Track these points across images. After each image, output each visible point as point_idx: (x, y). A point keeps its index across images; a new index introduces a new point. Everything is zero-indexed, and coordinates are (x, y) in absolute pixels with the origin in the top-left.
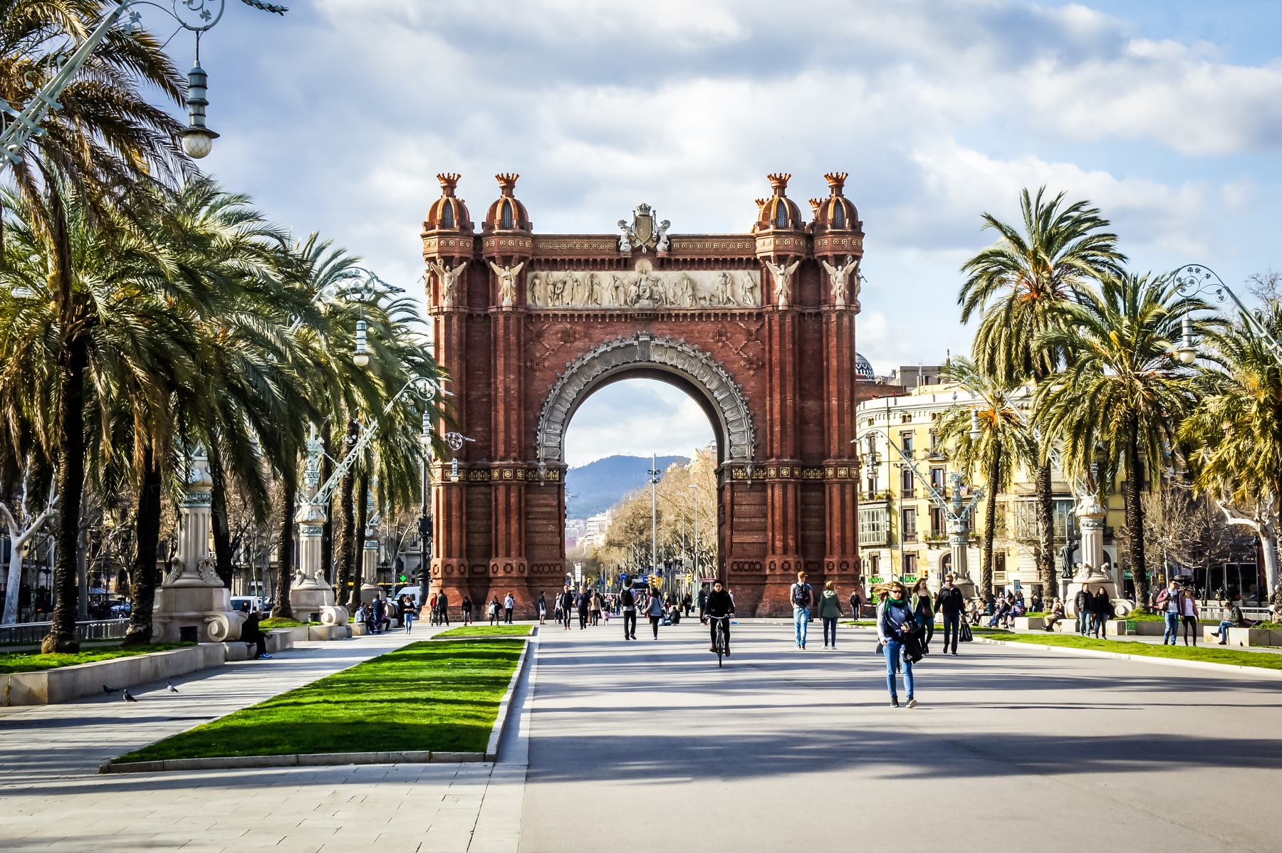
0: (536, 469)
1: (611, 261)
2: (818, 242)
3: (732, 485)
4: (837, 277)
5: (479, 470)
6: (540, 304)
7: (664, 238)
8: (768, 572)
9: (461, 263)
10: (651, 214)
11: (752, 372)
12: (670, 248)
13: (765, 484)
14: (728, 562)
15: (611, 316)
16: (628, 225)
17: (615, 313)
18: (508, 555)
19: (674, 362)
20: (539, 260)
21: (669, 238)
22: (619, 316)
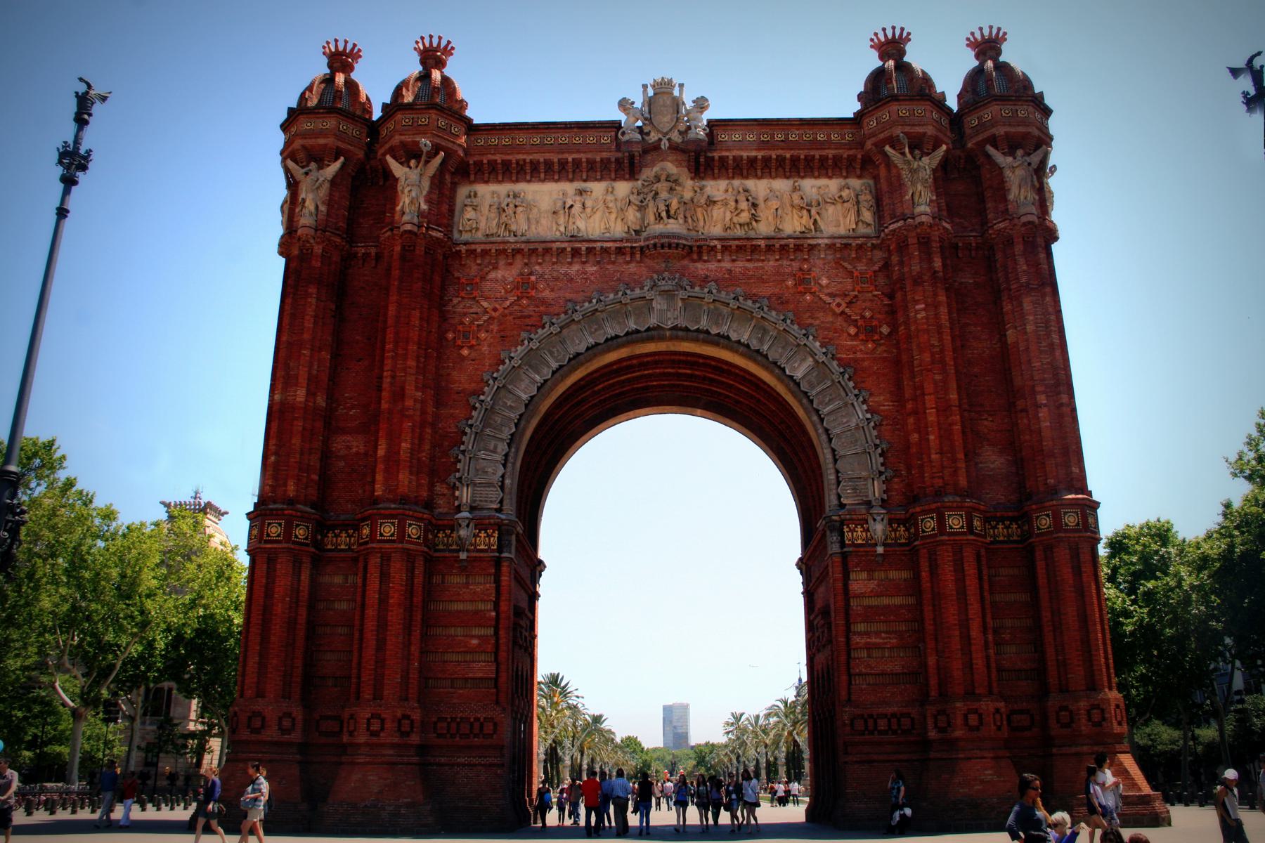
0: (454, 526)
1: (605, 163)
3: (844, 556)
4: (1013, 169)
5: (345, 526)
6: (479, 236)
8: (932, 734)
9: (336, 159)
10: (676, 93)
12: (711, 135)
14: (846, 714)
15: (605, 251)
16: (638, 105)
18: (378, 695)
19: (724, 330)
20: (479, 164)
21: (712, 124)
22: (620, 251)
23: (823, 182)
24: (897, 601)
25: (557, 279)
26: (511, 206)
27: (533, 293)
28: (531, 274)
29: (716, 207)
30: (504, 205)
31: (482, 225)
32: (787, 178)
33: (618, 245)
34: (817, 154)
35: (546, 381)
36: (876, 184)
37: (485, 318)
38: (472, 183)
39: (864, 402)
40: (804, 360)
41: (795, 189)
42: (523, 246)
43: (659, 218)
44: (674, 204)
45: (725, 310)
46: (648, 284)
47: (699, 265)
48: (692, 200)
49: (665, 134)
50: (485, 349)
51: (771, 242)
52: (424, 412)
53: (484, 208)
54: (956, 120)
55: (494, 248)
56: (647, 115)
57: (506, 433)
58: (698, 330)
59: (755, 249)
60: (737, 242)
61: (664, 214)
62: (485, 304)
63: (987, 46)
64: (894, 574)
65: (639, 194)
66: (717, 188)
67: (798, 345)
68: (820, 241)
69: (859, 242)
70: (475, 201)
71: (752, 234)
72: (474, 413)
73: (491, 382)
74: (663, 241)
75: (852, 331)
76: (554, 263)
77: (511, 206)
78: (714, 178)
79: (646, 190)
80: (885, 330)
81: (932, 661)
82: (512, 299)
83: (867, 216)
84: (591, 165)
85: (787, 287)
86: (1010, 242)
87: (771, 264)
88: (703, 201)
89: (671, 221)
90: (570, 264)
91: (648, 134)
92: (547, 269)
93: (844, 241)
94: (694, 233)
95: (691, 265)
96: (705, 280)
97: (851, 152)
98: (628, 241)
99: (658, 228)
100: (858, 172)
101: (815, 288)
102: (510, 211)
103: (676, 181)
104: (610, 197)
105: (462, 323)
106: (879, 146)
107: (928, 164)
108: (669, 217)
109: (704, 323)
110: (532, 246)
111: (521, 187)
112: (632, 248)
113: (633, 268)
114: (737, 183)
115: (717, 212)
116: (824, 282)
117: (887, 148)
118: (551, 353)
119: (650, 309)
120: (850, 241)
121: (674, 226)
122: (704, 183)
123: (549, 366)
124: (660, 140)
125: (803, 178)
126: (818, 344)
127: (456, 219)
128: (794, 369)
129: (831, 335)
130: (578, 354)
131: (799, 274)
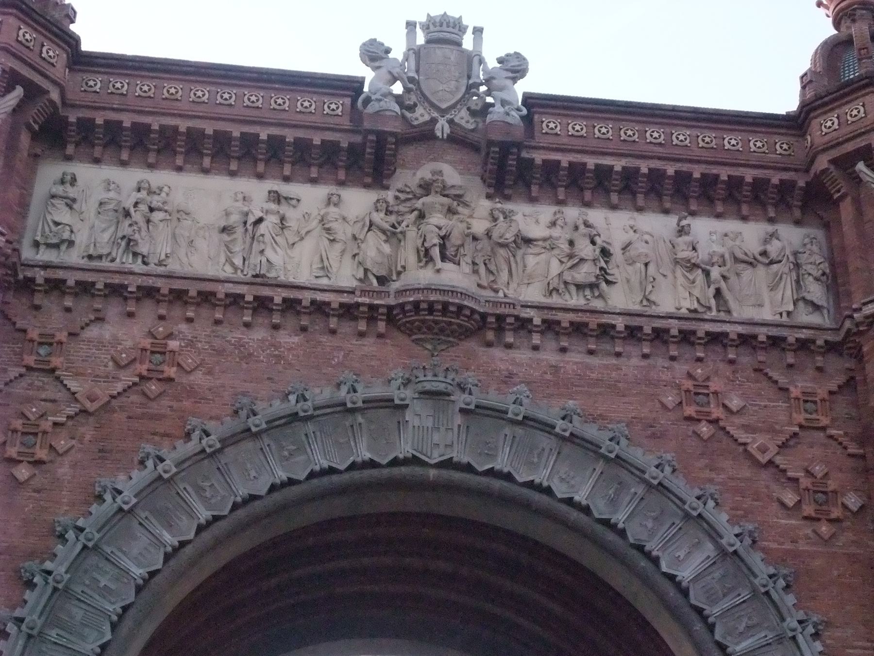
10: (468, 42)
11: (824, 529)
15: (320, 308)
16: (398, 53)
17: (335, 299)
19: (541, 477)
20: (86, 127)
22: (348, 311)
23: (731, 225)
25: (220, 352)
26: (143, 208)
27: (172, 372)
28: (170, 336)
29: (533, 250)
30: (129, 204)
31: (81, 238)
32: (666, 212)
33: (345, 299)
34: (724, 173)
35: (183, 544)
36: (829, 239)
37: (71, 411)
38: (68, 158)
39: (816, 636)
40: (697, 545)
41: (682, 231)
42: (159, 283)
43: (425, 256)
44: (455, 240)
45: (545, 441)
46: (399, 373)
47: (497, 352)
48: (488, 234)
49: (443, 112)
51: (635, 322)
53: (86, 207)
55: (100, 281)
56: (412, 74)
58: (491, 473)
59: (606, 331)
60: (571, 316)
61: (436, 252)
62: (73, 385)
65: (388, 212)
66: (533, 218)
67: (687, 516)
68: (727, 328)
69: (803, 334)
70: (72, 192)
71: (598, 304)
72: (28, 595)
73: (71, 535)
74: (433, 297)
75: (790, 498)
76: (218, 322)
77: (143, 208)
78: (533, 200)
79: (401, 208)
80: (853, 501)
82: (127, 378)
83: (816, 292)
84: (302, 148)
85: (664, 406)
87: (632, 363)
88: (510, 236)
89: (449, 266)
90: (247, 325)
91: (412, 108)
92: (202, 330)
93: (774, 332)
94: (488, 294)
95: (481, 350)
96: (508, 379)
97: (786, 176)
98: (364, 292)
100: (797, 213)
101: (717, 412)
102: (137, 216)
103: (458, 197)
104: (332, 209)
105: (23, 416)
106: (845, 163)
108: (444, 258)
109: (502, 463)
110: (177, 285)
112: (372, 308)
113: (369, 346)
114: (572, 213)
115: (533, 260)
116: (735, 403)
117: (861, 166)
118: (199, 490)
119: (401, 424)
120: (784, 332)
121: (454, 276)
122: (508, 206)
123: (191, 515)
124: (434, 121)
125: (693, 214)
126: (724, 517)
127: (31, 221)
128: (678, 561)
129: (748, 503)
130: (253, 498)
131: (688, 384)
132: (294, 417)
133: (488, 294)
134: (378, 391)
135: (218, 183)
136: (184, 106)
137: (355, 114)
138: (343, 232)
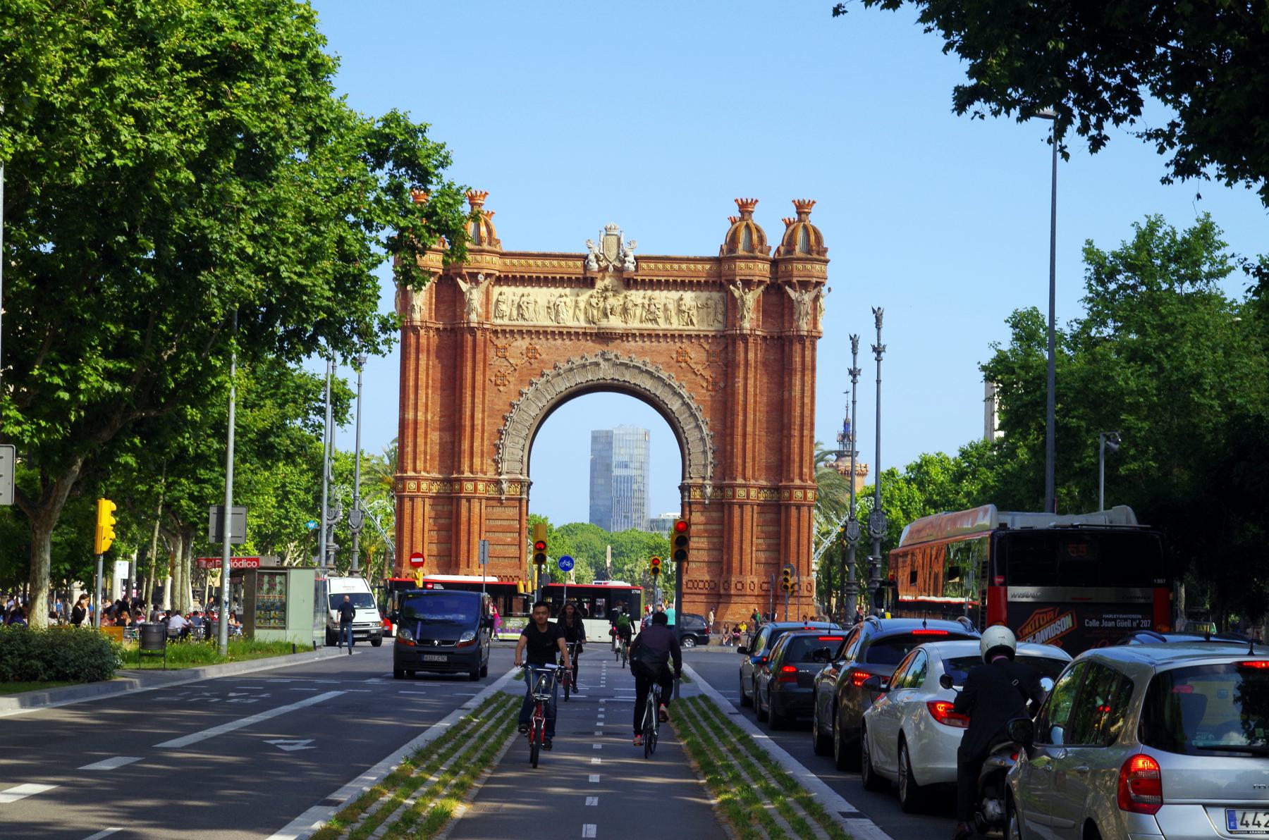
0: (498, 483)
2: (782, 267)
6: (506, 321)
7: (631, 258)
8: (722, 591)
12: (637, 267)
13: (723, 504)
15: (577, 334)
17: (581, 331)
20: (506, 277)
22: (585, 334)
23: (698, 293)
24: (714, 527)
34: (695, 280)
50: (512, 387)
52: (483, 425)
54: (774, 263)
57: (524, 434)
59: (657, 335)
63: (802, 208)
64: (714, 514)
66: (637, 296)
71: (655, 326)
80: (722, 385)
81: (725, 558)
83: (720, 318)
86: (791, 343)
96: (629, 352)
99: (604, 323)
107: (751, 299)
111: (528, 289)
113: (590, 344)
114: (649, 293)
116: (693, 356)
121: (615, 323)
132: (571, 369)
133: (623, 325)
134: (594, 360)
135: (544, 289)
136: (534, 268)
137: (586, 267)
138: (582, 305)
